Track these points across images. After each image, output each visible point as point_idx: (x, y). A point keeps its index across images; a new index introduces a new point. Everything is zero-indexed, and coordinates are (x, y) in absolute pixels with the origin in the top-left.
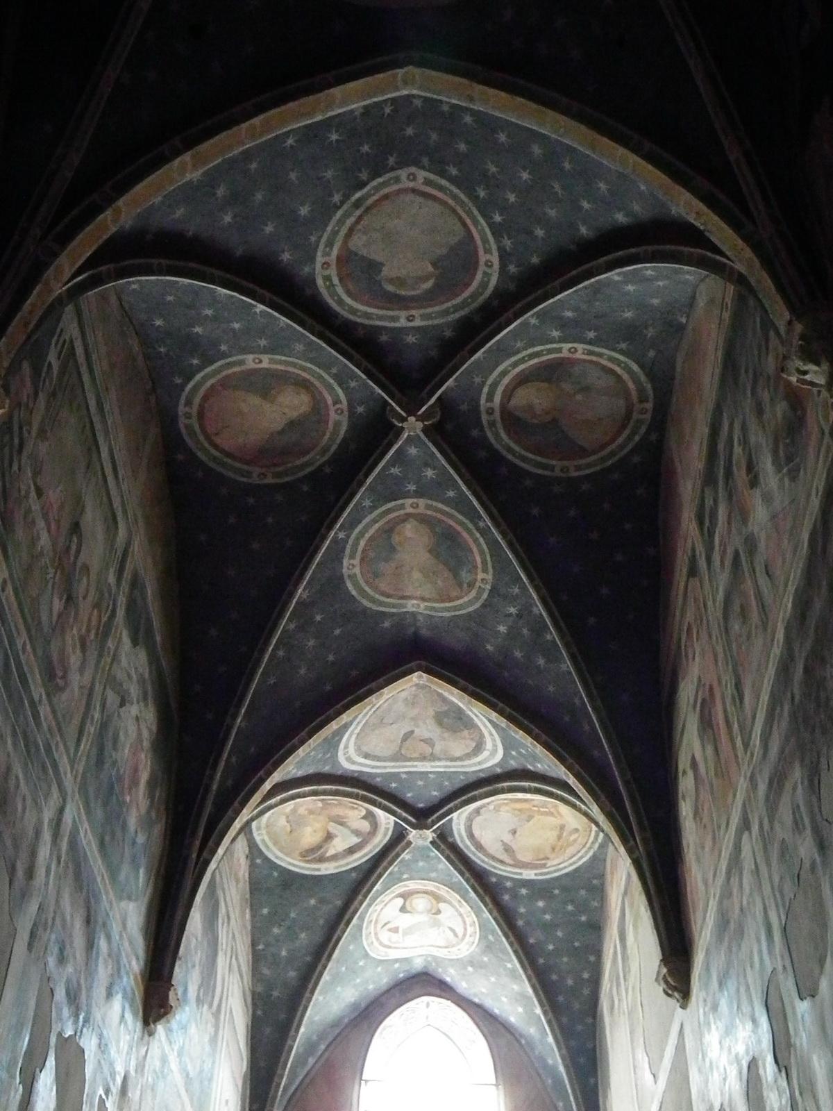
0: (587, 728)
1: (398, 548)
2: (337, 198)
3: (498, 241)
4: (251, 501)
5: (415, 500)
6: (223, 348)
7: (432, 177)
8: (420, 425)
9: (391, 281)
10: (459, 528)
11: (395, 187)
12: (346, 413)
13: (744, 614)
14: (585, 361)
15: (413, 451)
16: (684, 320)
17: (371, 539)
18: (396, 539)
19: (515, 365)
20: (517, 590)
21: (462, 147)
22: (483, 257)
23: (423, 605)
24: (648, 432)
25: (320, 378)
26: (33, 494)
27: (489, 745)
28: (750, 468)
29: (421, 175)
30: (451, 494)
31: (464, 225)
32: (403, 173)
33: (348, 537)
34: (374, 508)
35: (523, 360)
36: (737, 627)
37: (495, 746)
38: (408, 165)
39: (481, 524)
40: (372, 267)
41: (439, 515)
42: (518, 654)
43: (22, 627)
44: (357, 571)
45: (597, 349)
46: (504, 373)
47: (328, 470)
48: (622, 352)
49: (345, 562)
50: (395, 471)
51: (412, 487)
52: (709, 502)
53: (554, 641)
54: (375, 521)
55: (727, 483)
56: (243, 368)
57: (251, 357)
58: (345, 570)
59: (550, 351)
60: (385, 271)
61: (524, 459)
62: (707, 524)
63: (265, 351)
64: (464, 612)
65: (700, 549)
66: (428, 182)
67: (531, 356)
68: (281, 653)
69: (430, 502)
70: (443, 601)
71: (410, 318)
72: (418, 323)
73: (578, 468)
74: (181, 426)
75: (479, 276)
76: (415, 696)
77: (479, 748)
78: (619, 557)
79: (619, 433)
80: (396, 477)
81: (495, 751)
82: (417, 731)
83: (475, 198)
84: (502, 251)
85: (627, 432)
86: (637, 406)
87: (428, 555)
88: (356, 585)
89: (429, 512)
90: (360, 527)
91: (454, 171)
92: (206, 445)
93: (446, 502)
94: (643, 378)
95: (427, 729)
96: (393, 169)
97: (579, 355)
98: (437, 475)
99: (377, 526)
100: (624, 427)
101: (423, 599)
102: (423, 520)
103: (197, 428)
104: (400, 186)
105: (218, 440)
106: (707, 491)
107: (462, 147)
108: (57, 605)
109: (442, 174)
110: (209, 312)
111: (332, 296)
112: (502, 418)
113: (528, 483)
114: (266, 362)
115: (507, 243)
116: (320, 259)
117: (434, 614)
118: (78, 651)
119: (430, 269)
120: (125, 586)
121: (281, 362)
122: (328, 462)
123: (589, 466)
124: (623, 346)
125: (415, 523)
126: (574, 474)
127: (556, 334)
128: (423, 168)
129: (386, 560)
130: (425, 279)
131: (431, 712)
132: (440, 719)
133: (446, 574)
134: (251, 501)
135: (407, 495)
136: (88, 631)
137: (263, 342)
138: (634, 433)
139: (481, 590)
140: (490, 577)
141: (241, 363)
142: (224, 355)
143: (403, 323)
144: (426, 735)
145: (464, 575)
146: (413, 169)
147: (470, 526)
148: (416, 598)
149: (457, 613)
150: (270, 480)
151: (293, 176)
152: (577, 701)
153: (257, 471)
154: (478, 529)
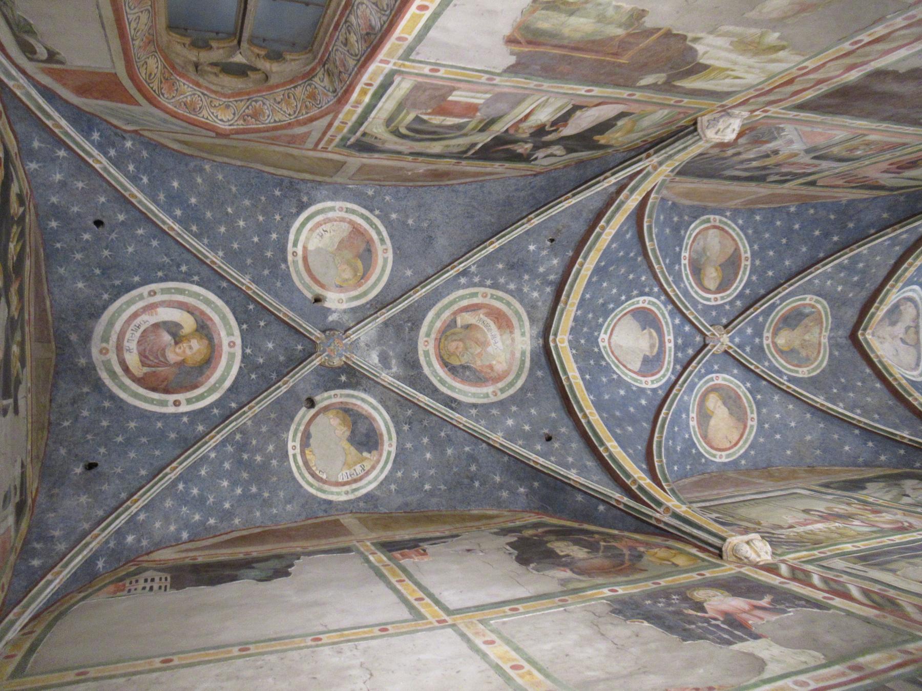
0: (904, 236)
1: (791, 347)
2: (615, 376)
3: (634, 297)
4: (766, 426)
5: (764, 339)
6: (687, 436)
7: (603, 331)
8: (725, 336)
9: (652, 353)
10: (780, 314)
11: (608, 349)
12: (718, 375)
13: (851, 150)
14: (690, 252)
15: (737, 340)
16: (670, 203)
17: (787, 362)
18: (785, 349)
19: (692, 287)
20: (817, 281)
21: (590, 316)
22: (641, 305)
23: (824, 333)
24: (726, 217)
25: (701, 388)
26: (794, 530)
27: (910, 294)
28: (767, 156)
29: (602, 336)
30: (761, 319)
31: (625, 314)
32: (601, 344)
33: (786, 374)
34: (770, 361)
35: (690, 284)
36: (859, 152)
37: (911, 290)
38: (598, 343)
39: (778, 302)
40: (646, 361)
41: (773, 325)
42: (856, 279)
43: (878, 540)
44: (805, 369)
45: (684, 246)
46: (696, 292)
47: (748, 385)
48: (686, 233)
49: (800, 376)
50: (748, 349)
51: (757, 340)
52: (777, 178)
53: (850, 258)
54: (776, 360)
55: (769, 168)
56: (696, 427)
57: (691, 423)
58: (806, 376)
59: (685, 270)
60: (647, 354)
61: (741, 281)
62: (788, 177)
63: (688, 415)
64: (829, 310)
65: (801, 181)
66: (605, 333)
67: (688, 279)
68: (859, 411)
69: (765, 330)
70: (821, 323)
71: (670, 341)
72: (672, 338)
73: (746, 252)
74: (727, 460)
75: (649, 306)
76: (879, 337)
77: (910, 299)
78: (797, 226)
79: (727, 232)
80: (752, 348)
81: (914, 290)
82: (901, 336)
83: (613, 310)
84: (637, 296)
85: (727, 228)
86: (713, 223)
87: (796, 331)
88: (814, 370)
89: (771, 330)
90: (781, 368)
91: (601, 320)
92: (736, 448)
93: (765, 321)
94: (697, 222)
95: (899, 329)
96: (600, 349)
97: (687, 255)
98: (750, 327)
99: (779, 359)
100: (723, 229)
101: (821, 333)
102: (775, 334)
103: (728, 452)
104: (607, 345)
105: (734, 442)
106: (768, 180)
107: (590, 316)
108: (856, 523)
109: (601, 325)
110: (670, 442)
111: (661, 380)
112: (720, 293)
113: (754, 278)
114: (693, 415)
115: (635, 292)
116: (644, 386)
117: (829, 327)
118: (884, 514)
119: (645, 331)
120: (830, 491)
121: (693, 407)
122: (744, 384)
123: (744, 247)
124: (682, 232)
125: (777, 337)
126: (749, 254)
127: (677, 267)
128: (599, 335)
129: (799, 353)
130: (650, 334)
131: (889, 328)
132: (893, 324)
133: (806, 321)
134: (766, 426)
135: (761, 342)
136: (866, 510)
137: (684, 416)
138: (726, 224)
139: (817, 301)
140: (809, 296)
141: (694, 427)
142: (690, 436)
143: (672, 345)
144: (903, 330)
145: (807, 311)
146: (599, 340)
147: (779, 308)
148: (820, 337)
149: (829, 314)
150: (755, 416)
151: (607, 397)
152: (887, 243)
153: (749, 423)
154: (780, 304)
